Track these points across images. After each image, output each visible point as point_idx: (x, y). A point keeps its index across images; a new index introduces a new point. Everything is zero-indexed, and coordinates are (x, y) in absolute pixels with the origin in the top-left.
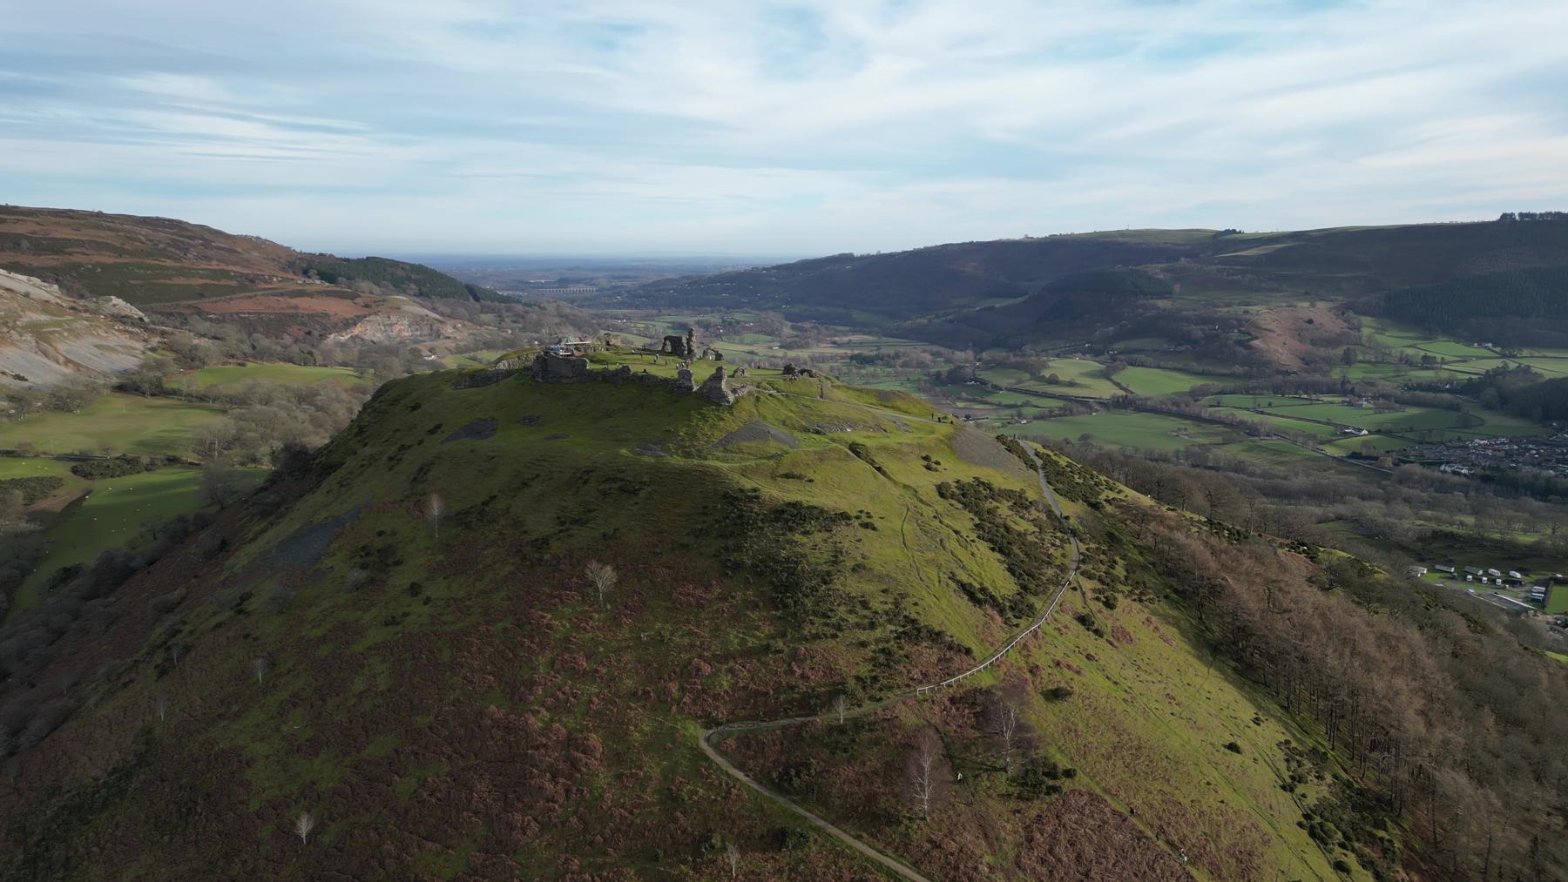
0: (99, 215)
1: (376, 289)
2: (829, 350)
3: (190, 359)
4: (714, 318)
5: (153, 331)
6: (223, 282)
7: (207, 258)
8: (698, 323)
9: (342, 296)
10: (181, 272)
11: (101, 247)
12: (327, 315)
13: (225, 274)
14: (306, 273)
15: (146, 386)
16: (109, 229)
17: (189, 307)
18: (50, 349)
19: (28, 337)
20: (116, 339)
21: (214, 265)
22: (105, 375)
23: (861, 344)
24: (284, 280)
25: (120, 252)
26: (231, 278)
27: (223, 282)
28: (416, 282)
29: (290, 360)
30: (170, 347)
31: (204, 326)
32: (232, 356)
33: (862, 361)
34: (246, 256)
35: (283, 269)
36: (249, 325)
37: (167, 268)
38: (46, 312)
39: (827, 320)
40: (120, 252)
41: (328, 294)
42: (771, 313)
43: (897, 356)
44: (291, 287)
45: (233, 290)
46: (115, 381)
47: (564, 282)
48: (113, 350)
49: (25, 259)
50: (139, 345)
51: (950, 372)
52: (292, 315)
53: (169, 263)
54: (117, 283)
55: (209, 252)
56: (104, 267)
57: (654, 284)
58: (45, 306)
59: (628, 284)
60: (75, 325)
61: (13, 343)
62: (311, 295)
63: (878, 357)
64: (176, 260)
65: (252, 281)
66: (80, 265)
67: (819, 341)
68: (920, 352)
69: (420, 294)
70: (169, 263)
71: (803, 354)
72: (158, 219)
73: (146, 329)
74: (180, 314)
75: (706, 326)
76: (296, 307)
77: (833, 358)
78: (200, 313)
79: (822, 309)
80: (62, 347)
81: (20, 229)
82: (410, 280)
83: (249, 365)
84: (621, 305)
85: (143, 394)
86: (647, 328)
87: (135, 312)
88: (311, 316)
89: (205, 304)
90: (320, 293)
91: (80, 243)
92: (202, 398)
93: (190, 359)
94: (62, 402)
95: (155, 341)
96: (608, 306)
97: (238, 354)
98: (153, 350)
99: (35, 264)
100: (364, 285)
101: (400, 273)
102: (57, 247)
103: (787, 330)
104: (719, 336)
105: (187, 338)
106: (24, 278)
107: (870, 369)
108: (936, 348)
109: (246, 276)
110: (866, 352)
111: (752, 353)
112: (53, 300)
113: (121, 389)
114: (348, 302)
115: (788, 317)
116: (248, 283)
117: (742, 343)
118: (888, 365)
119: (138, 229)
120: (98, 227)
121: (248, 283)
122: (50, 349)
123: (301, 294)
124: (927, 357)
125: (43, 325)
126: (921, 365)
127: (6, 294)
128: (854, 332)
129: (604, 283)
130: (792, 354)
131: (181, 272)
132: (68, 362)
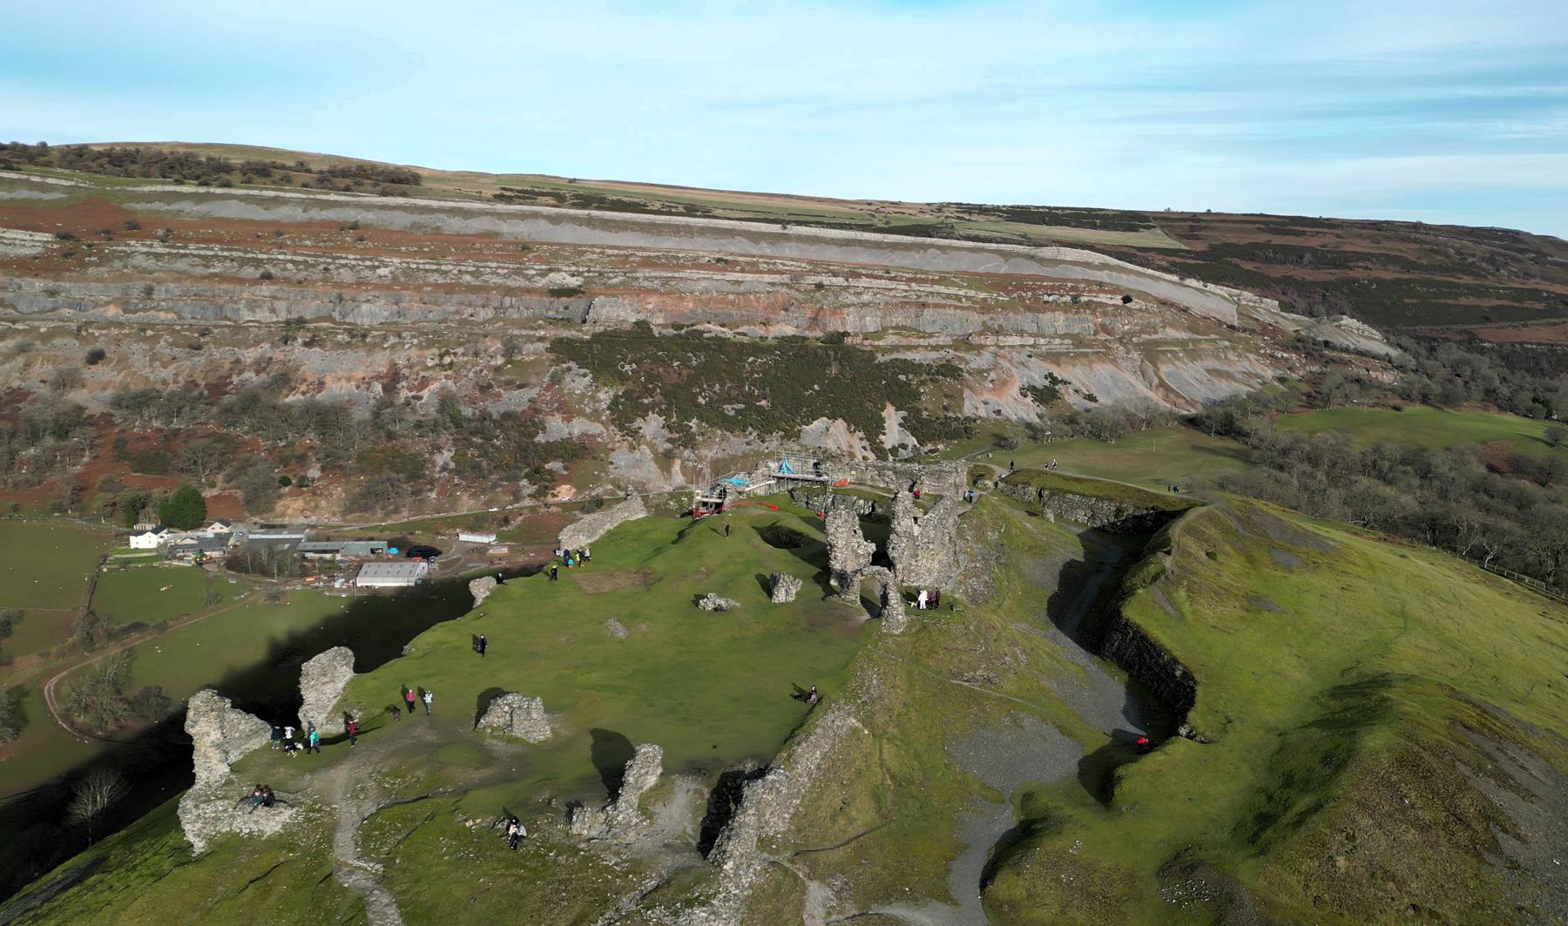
0: (1417, 227)
6: (1527, 304)
7: (1528, 275)
10: (1476, 291)
11: (1388, 260)
13: (1535, 294)
16: (1416, 241)
19: (1135, 355)
21: (1531, 284)
26: (1540, 299)
27: (1527, 304)
29: (1509, 406)
36: (1510, 359)
37: (1458, 286)
38: (1190, 329)
40: (1408, 265)
45: (1534, 314)
48: (1229, 376)
50: (1269, 373)
53: (1467, 280)
54: (1388, 302)
56: (1379, 281)
61: (1114, 362)
64: (1478, 275)
66: (1355, 280)
70: (1467, 280)
78: (1471, 343)
80: (1165, 369)
81: (1314, 242)
83: (1414, 409)
94: (1096, 428)
98: (1282, 380)
99: (1309, 278)
102: (1341, 260)
113: (1192, 422)
120: (1405, 240)
127: (1154, 307)
131: (1476, 291)
132: (1162, 384)
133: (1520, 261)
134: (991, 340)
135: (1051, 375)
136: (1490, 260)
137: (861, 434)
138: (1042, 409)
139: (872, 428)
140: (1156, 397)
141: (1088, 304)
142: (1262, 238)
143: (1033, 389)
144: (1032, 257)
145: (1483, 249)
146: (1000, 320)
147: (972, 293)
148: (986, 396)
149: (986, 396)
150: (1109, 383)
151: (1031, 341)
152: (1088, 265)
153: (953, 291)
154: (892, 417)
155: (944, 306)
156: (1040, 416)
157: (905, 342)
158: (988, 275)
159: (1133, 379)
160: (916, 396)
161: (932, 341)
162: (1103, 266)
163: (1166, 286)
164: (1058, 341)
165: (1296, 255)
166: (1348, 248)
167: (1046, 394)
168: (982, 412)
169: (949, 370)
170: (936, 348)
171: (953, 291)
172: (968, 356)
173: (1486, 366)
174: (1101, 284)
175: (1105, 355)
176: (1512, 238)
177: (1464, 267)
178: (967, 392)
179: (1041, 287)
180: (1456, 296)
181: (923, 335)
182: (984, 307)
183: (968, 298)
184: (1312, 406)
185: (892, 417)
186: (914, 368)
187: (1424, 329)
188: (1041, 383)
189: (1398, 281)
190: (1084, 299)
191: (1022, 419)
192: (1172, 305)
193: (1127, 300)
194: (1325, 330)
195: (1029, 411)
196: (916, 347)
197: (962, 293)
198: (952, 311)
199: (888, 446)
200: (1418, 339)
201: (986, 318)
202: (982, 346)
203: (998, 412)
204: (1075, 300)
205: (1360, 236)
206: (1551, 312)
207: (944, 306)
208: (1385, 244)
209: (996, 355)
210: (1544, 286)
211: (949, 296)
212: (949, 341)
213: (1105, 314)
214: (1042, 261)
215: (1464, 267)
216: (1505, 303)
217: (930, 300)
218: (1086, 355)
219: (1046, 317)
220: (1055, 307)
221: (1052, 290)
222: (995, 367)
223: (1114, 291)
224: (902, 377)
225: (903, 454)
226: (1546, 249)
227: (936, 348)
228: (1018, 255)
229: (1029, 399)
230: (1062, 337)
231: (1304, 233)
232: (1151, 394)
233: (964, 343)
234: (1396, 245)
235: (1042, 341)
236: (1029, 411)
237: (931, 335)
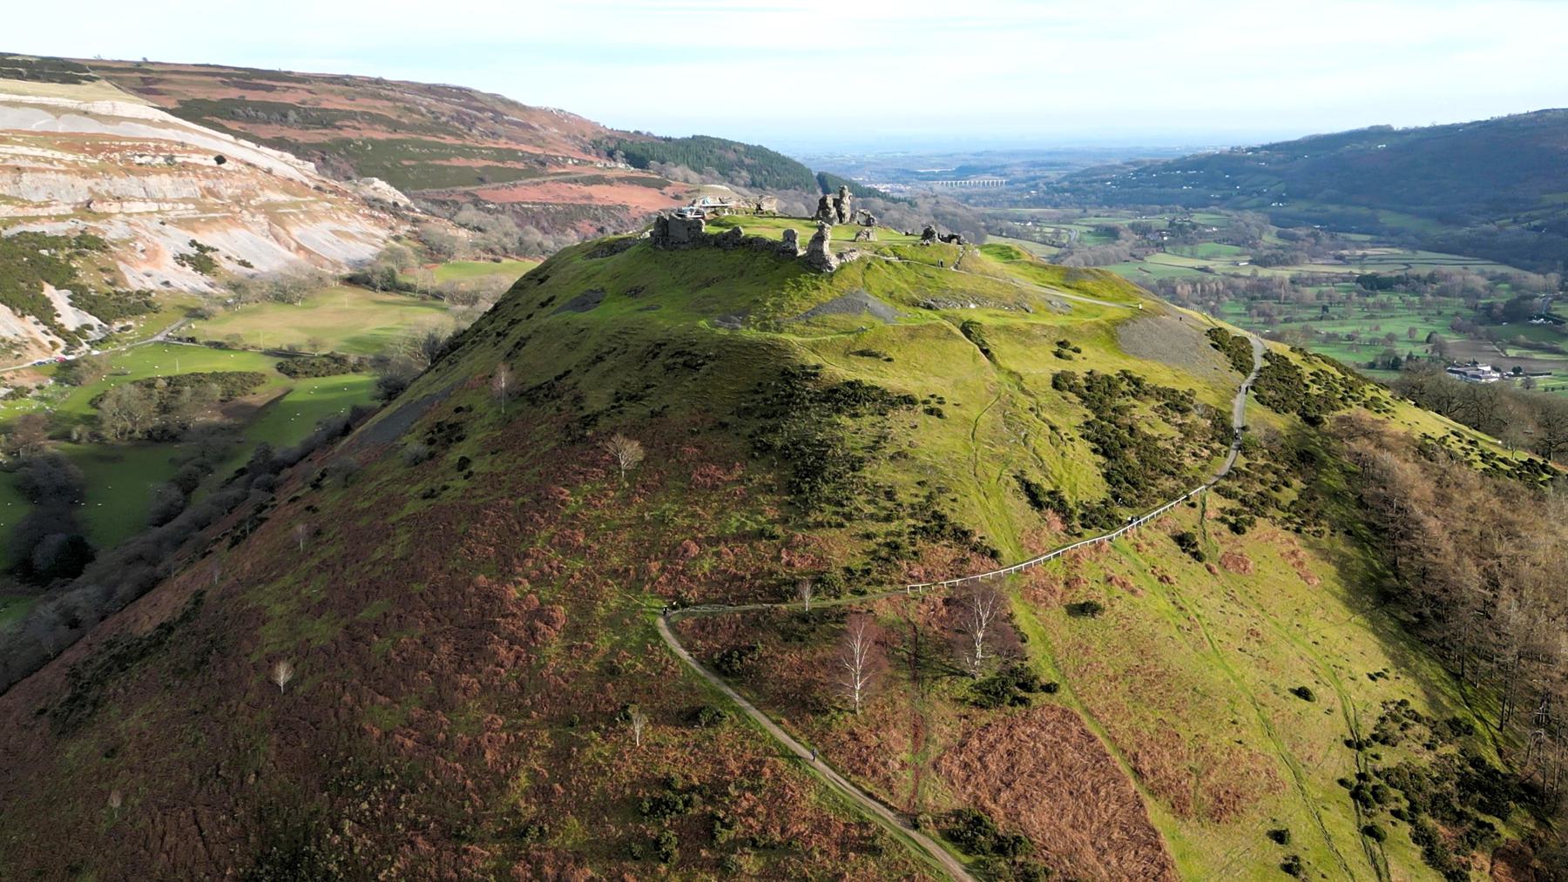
0: (379, 82)
1: (693, 176)
2: (1321, 268)
3: (435, 252)
4: (1161, 221)
5: (404, 218)
6: (509, 164)
8: (1133, 227)
9: (647, 184)
11: (375, 119)
12: (625, 208)
13: (512, 154)
14: (611, 155)
15: (376, 279)
17: (466, 193)
18: (282, 232)
19: (260, 218)
20: (359, 224)
21: (502, 144)
22: (336, 264)
23: (1380, 260)
24: (581, 162)
25: (395, 126)
26: (518, 159)
27: (509, 164)
28: (749, 169)
30: (417, 237)
31: (469, 214)
32: (492, 251)
33: (1373, 284)
34: (542, 133)
35: (585, 151)
36: (526, 216)
37: (445, 146)
38: (286, 191)
39: (1336, 226)
40: (395, 126)
41: (630, 181)
42: (1249, 216)
43: (1432, 279)
44: (588, 172)
45: (518, 175)
46: (346, 272)
47: (964, 171)
48: (351, 236)
49: (291, 134)
51: (1509, 304)
52: (583, 208)
53: (449, 140)
55: (498, 128)
56: (375, 143)
57: (1084, 173)
58: (287, 185)
59: (1053, 175)
60: (315, 207)
61: (244, 225)
62: (609, 182)
63: (1399, 280)
65: (543, 164)
66: (349, 142)
67: (1314, 255)
68: (1475, 274)
69: (753, 185)
70: (449, 140)
71: (1285, 273)
72: (445, 87)
73: (396, 215)
74: (455, 203)
75: (1143, 231)
76: (590, 197)
77: (1330, 279)
78: (477, 202)
79: (1334, 209)
80: (296, 231)
81: (289, 98)
82: (741, 165)
83: (505, 261)
84: (1036, 202)
85: (374, 287)
86: (1057, 234)
87: (403, 200)
88: (606, 209)
89: (485, 192)
90: (620, 179)
91: (351, 115)
92: (438, 296)
93: (435, 252)
94: (283, 293)
95: (403, 229)
96: (1014, 203)
97: (497, 248)
98: (397, 239)
99: (301, 140)
100: (679, 171)
101: (731, 156)
102: (326, 120)
103: (1269, 238)
104: (1160, 246)
105: (441, 228)
106: (276, 153)
107: (1383, 296)
108: (1501, 269)
109: (536, 158)
110: (1384, 271)
111: (1205, 270)
112: (297, 176)
113: (351, 281)
114: (656, 191)
115: (1276, 220)
116: (538, 167)
117: (1193, 255)
118: (1414, 292)
119: (419, 99)
121: (538, 167)
122: (282, 232)
123: (597, 180)
124: (1480, 283)
125: (278, 205)
126: (1469, 293)
127: (246, 170)
128: (1376, 244)
129: (1019, 173)
130: (1264, 273)
132: (300, 248)
133: (482, 120)
134: (115, 208)
135: (193, 243)
136: (459, 117)
137: (33, 318)
138: (207, 278)
139: (45, 313)
140: (300, 258)
141: (184, 165)
142: (234, 93)
143: (189, 259)
144: (86, 113)
145: (446, 107)
146: (104, 186)
147: (58, 155)
148: (146, 268)
149: (146, 268)
150: (248, 246)
151: (154, 207)
152: (149, 122)
153: (38, 152)
154: (59, 299)
155: (43, 171)
156: (212, 285)
157: (21, 213)
158: (45, 133)
159: (267, 242)
160: (72, 273)
161: (52, 211)
162: (164, 124)
163: (223, 143)
164: (182, 206)
165: (280, 113)
166: (325, 105)
167: (201, 260)
168: (149, 285)
169: (86, 243)
170: (60, 218)
171: (38, 152)
172: (101, 225)
173: (509, 223)
174: (183, 144)
175: (233, 220)
176: (464, 94)
177: (438, 127)
178: (122, 266)
179: (121, 149)
180: (447, 157)
181: (26, 203)
182: (85, 173)
183: (59, 161)
184: (436, 261)
185: (59, 299)
186: (55, 242)
187: (430, 192)
188: (193, 251)
189: (390, 142)
190: (179, 160)
191: (193, 289)
192: (254, 166)
193: (220, 160)
194: (368, 191)
195: (190, 281)
196: (38, 218)
197: (49, 154)
198: (54, 176)
199: (71, 327)
200: (434, 202)
201: (90, 182)
202: (107, 215)
203: (167, 283)
204: (170, 159)
205: (332, 91)
206: (529, 173)
207: (43, 171)
208: (359, 101)
209: (129, 224)
210: (513, 146)
211: (36, 159)
212: (69, 210)
213: (207, 176)
214: (98, 117)
215: (438, 127)
216: (490, 163)
217: (21, 164)
218: (215, 220)
219: (152, 180)
220: (156, 170)
221: (141, 150)
222: (136, 237)
223: (198, 151)
224: (45, 252)
225: (95, 335)
226: (500, 108)
227: (60, 218)
228: (67, 110)
229: (189, 269)
230: (184, 200)
231: (272, 89)
232: (292, 256)
233: (85, 210)
234: (369, 102)
235: (167, 207)
236: (190, 281)
237: (48, 205)
